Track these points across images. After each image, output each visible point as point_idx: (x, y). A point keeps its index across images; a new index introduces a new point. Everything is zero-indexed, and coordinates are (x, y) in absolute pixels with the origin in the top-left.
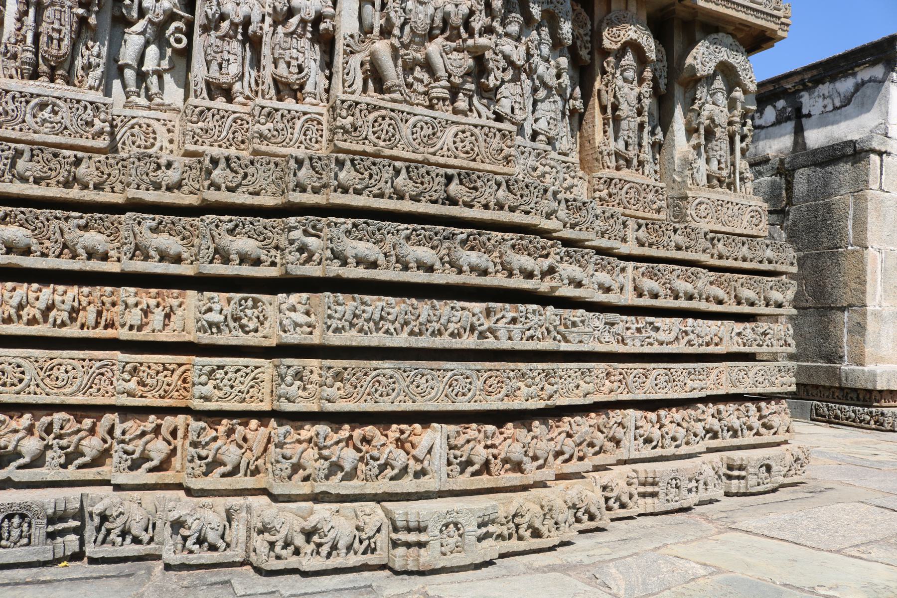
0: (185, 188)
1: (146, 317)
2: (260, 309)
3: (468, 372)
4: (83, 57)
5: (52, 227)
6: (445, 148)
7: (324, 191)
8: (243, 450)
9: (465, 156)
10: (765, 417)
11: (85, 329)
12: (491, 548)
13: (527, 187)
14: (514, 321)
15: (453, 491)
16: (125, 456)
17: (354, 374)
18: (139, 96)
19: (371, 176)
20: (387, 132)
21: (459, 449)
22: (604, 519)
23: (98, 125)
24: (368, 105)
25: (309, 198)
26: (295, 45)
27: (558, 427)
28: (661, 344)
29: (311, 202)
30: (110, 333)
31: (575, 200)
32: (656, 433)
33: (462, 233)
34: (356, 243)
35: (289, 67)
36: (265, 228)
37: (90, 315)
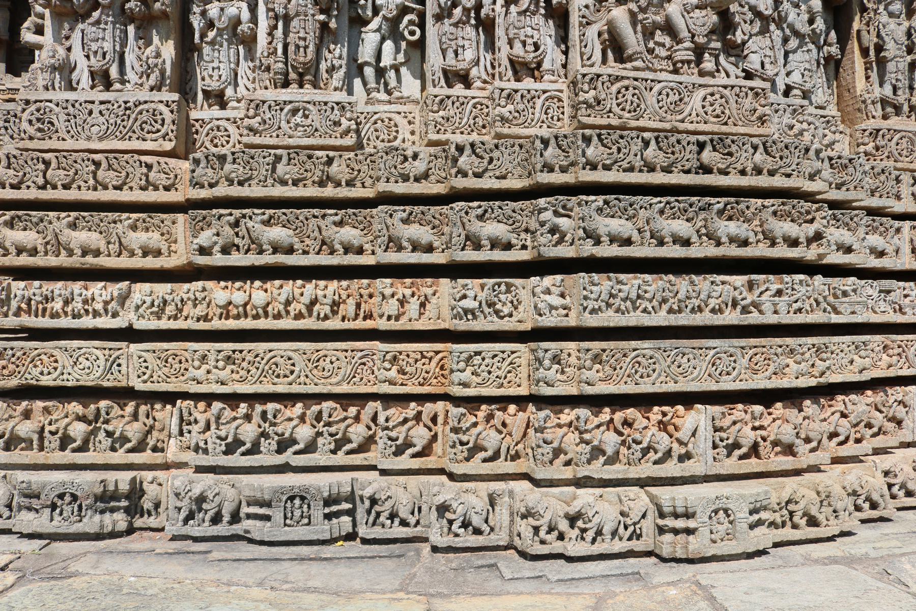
0: (432, 177)
1: (403, 307)
2: (513, 293)
3: (732, 350)
4: (326, 60)
5: (311, 226)
6: (694, 113)
7: (572, 169)
8: (503, 436)
11: (346, 322)
12: (763, 537)
13: (787, 147)
14: (779, 293)
15: (720, 475)
16: (389, 442)
17: (613, 356)
18: (379, 92)
19: (619, 150)
20: (632, 103)
21: (725, 431)
22: (888, 508)
23: (345, 123)
24: (610, 76)
25: (557, 178)
26: (529, 23)
27: (830, 406)
29: (560, 182)
30: (369, 324)
31: (839, 157)
33: (718, 203)
34: (608, 221)
35: (524, 46)
36: (514, 211)
37: (349, 308)
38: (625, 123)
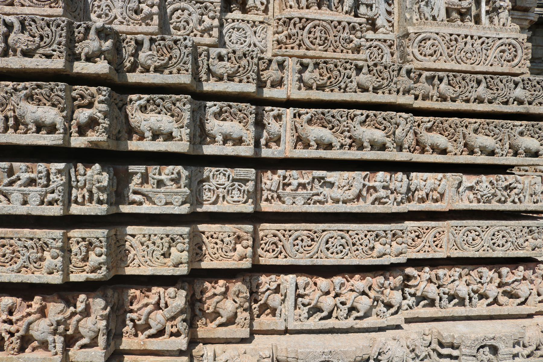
10: (507, 284)
13: (48, 26)
14: (32, 182)
28: (337, 201)
32: (328, 302)
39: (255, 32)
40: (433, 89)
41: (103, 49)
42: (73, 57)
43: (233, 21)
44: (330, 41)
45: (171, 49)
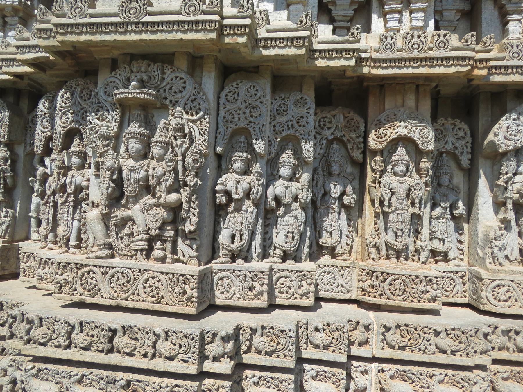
9: (150, 299)
13: (186, 337)
24: (77, 264)
31: (272, 328)
38: (83, 299)
39: (342, 275)
40: (509, 340)
41: (226, 351)
42: (203, 357)
43: (325, 266)
44: (408, 293)
45: (279, 337)
